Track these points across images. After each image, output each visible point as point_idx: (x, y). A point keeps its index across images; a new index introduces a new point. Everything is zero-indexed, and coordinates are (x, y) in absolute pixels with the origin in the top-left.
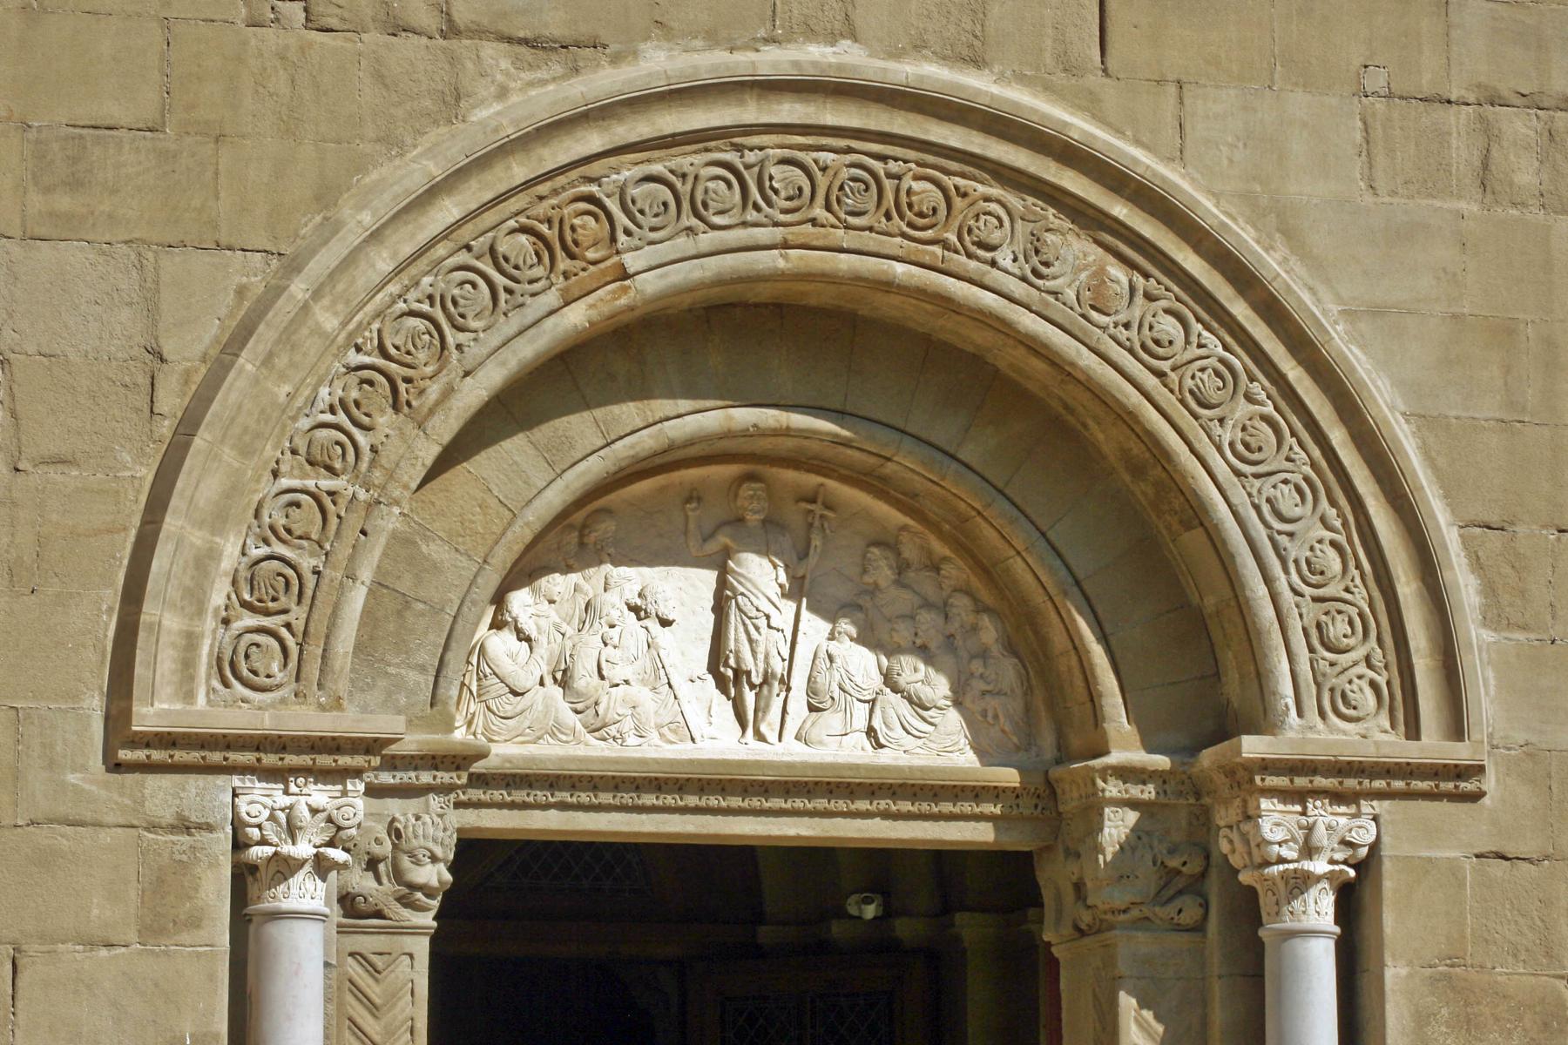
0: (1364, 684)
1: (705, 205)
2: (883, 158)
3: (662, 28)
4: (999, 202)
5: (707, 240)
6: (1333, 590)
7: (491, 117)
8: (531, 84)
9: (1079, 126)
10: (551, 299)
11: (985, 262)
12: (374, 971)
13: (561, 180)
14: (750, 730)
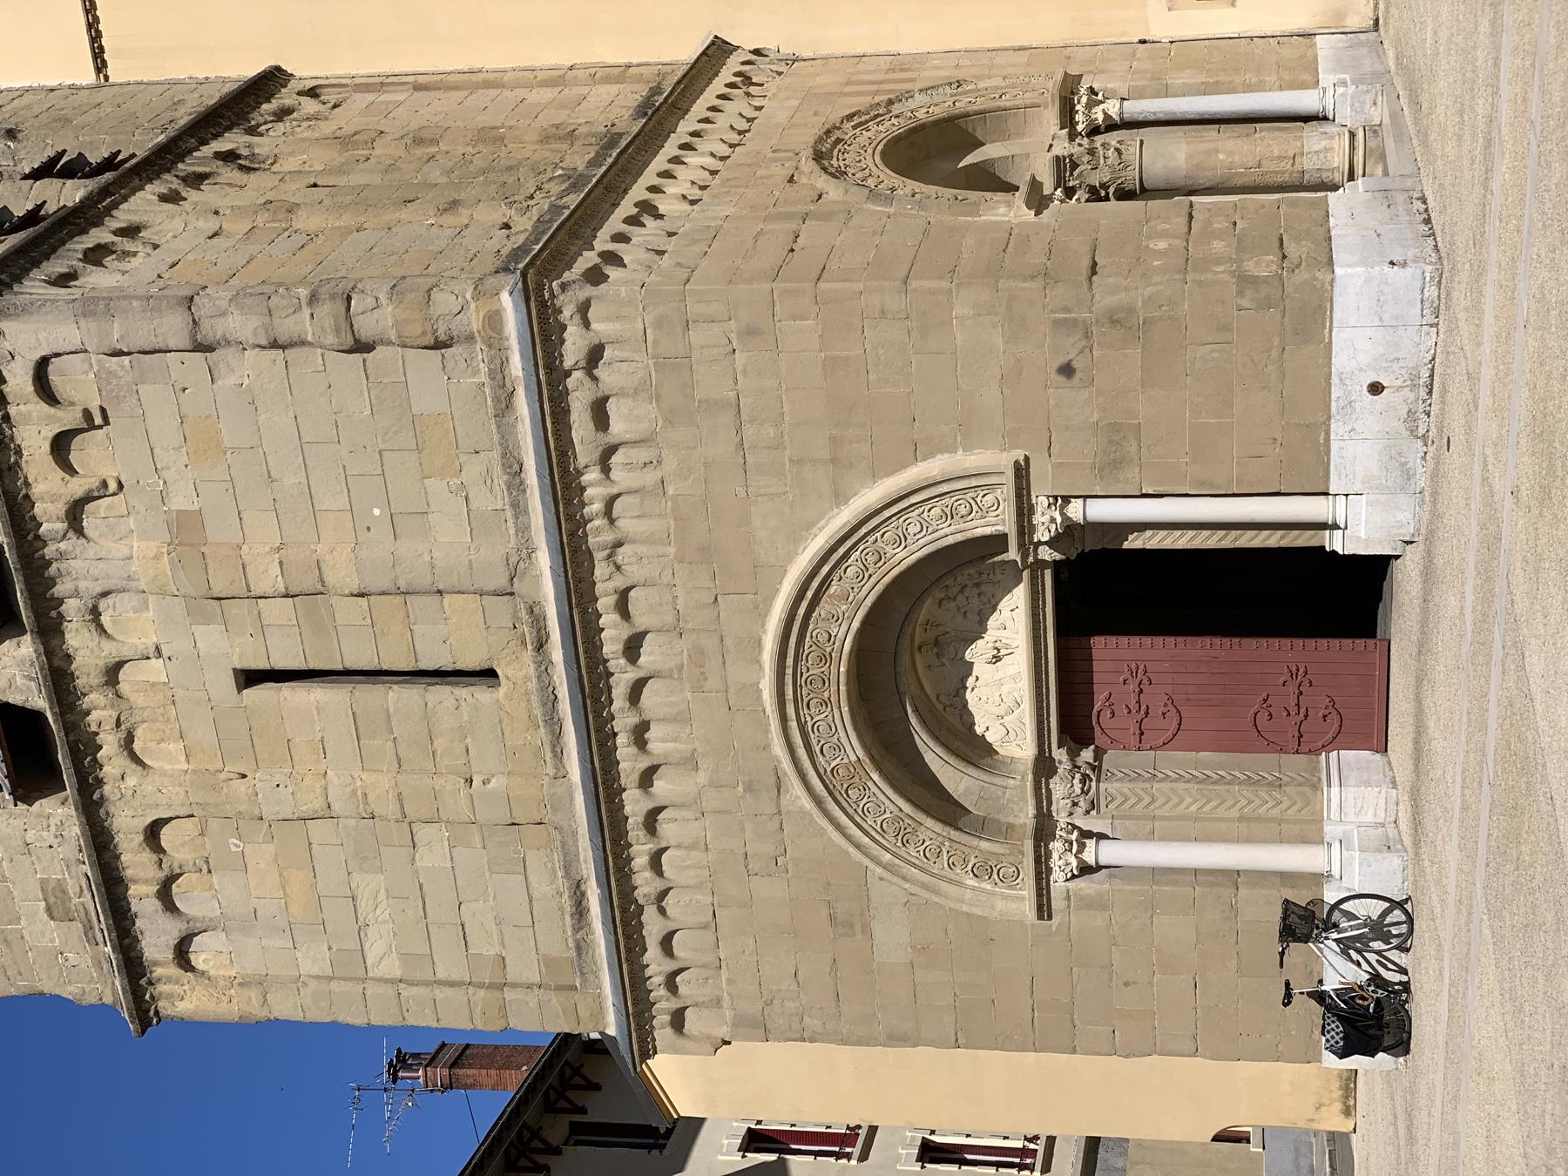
3: (767, 747)
5: (842, 734)
6: (948, 511)
7: (807, 803)
10: (870, 784)
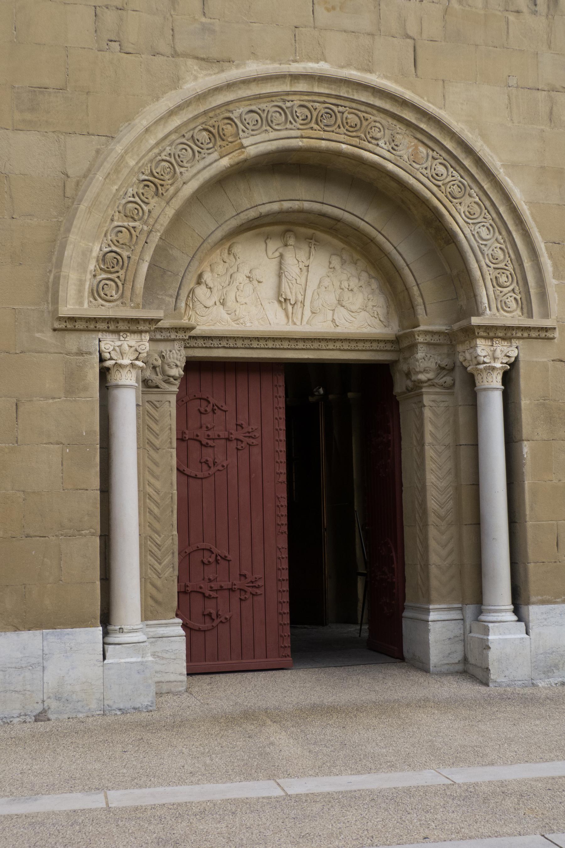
0: (512, 299)
1: (272, 121)
2: (337, 105)
3: (254, 55)
4: (379, 122)
6: (502, 265)
8: (206, 75)
9: (408, 95)
10: (215, 155)
11: (375, 145)
12: (155, 407)
13: (218, 111)
14: (290, 320)
